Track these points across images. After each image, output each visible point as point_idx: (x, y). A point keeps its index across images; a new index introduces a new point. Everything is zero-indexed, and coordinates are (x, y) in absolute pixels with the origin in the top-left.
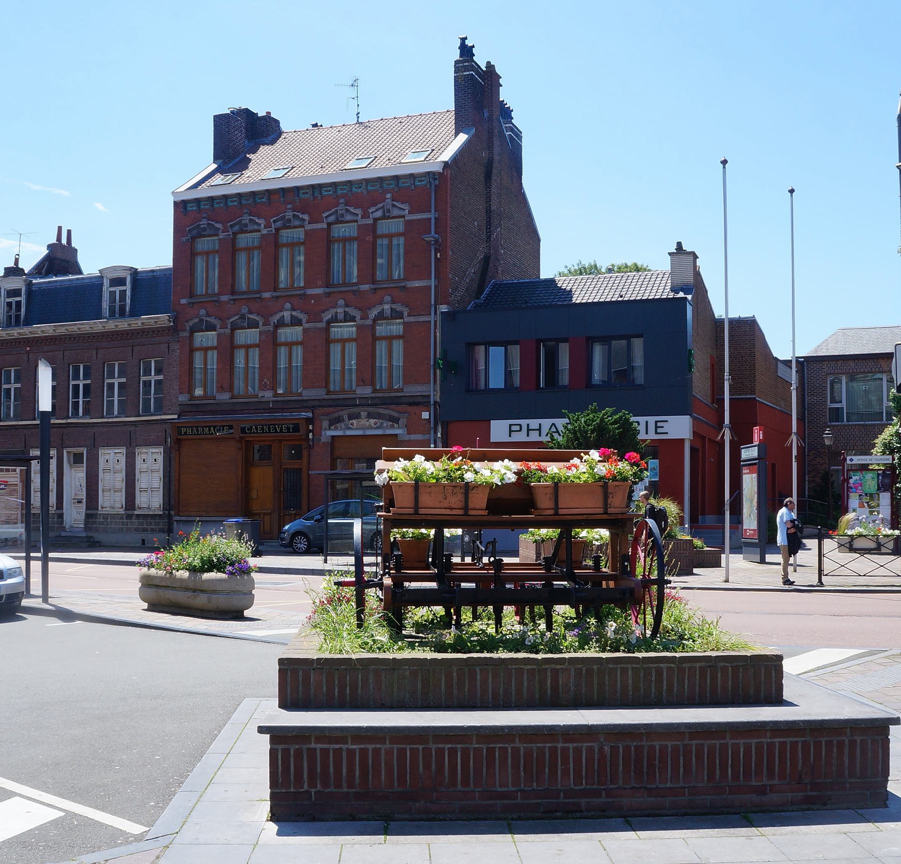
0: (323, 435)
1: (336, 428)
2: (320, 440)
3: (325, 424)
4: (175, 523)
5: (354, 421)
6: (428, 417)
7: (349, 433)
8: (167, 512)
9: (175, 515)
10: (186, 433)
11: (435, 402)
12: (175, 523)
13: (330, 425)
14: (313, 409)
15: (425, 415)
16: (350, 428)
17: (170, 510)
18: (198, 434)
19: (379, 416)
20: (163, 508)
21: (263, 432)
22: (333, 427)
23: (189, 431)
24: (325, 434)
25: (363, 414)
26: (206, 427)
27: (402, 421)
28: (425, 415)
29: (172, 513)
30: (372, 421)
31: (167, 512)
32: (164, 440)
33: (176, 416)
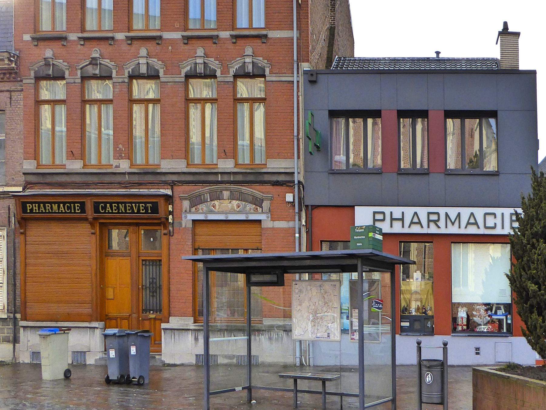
0: (183, 219)
1: (197, 212)
2: (181, 224)
3: (186, 204)
4: (22, 330)
5: (216, 203)
6: (292, 200)
7: (211, 217)
8: (12, 315)
9: (22, 320)
10: (31, 210)
11: (299, 182)
12: (22, 330)
13: (191, 206)
14: (172, 185)
15: (289, 197)
16: (211, 212)
17: (15, 312)
18: (46, 213)
19: (241, 197)
20: (8, 310)
21: (118, 213)
22: (193, 209)
23: (36, 208)
24: (186, 217)
25: (226, 194)
26: (55, 203)
27: (266, 204)
28: (289, 197)
29: (18, 316)
30: (235, 203)
31: (12, 315)
32: (7, 219)
33: (20, 189)
